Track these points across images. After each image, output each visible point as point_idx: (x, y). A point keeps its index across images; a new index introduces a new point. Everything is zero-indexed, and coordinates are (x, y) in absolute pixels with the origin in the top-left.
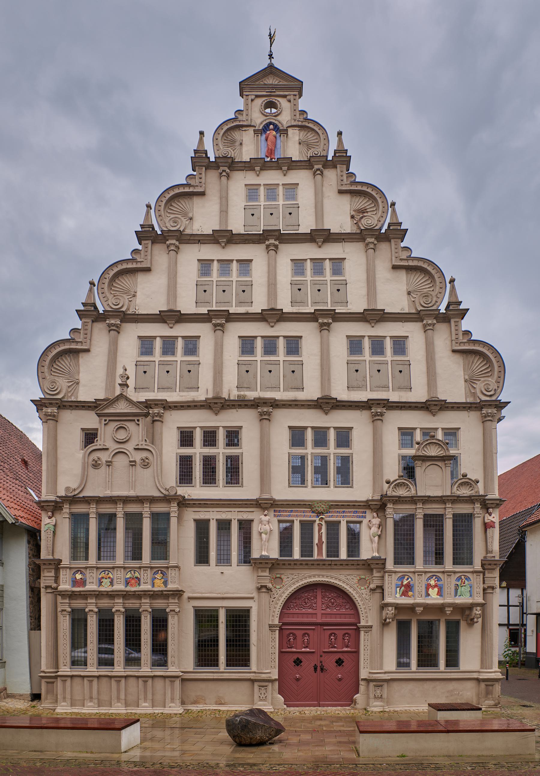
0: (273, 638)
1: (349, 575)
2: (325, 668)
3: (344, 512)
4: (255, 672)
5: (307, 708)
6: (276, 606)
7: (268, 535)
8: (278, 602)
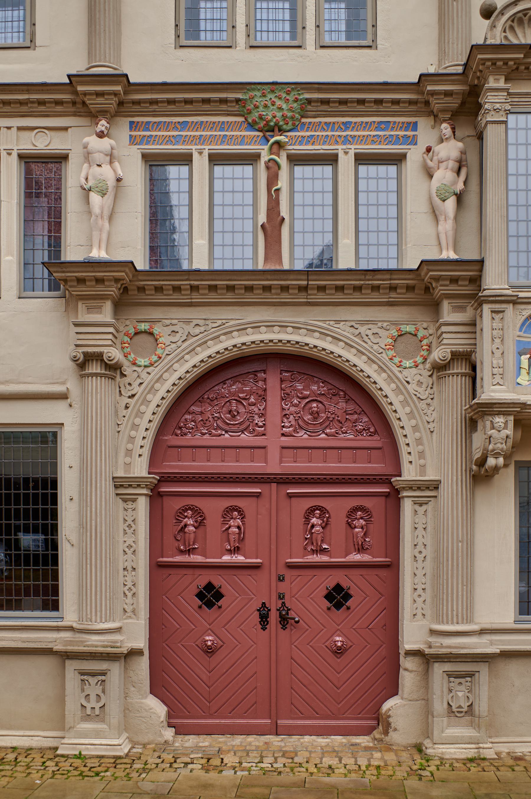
0: (129, 522)
1: (363, 323)
2: (292, 614)
3: (346, 126)
4: (71, 629)
5: (238, 740)
6: (137, 421)
7: (109, 198)
8: (143, 408)
